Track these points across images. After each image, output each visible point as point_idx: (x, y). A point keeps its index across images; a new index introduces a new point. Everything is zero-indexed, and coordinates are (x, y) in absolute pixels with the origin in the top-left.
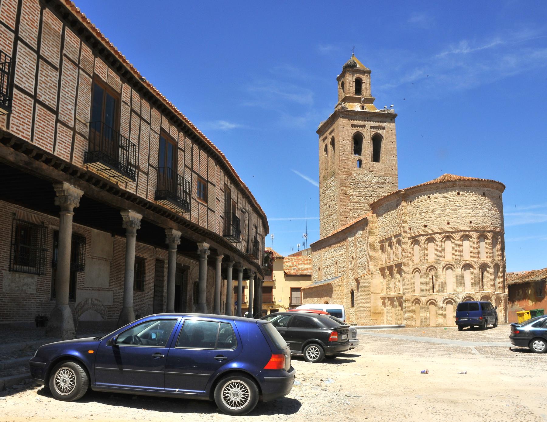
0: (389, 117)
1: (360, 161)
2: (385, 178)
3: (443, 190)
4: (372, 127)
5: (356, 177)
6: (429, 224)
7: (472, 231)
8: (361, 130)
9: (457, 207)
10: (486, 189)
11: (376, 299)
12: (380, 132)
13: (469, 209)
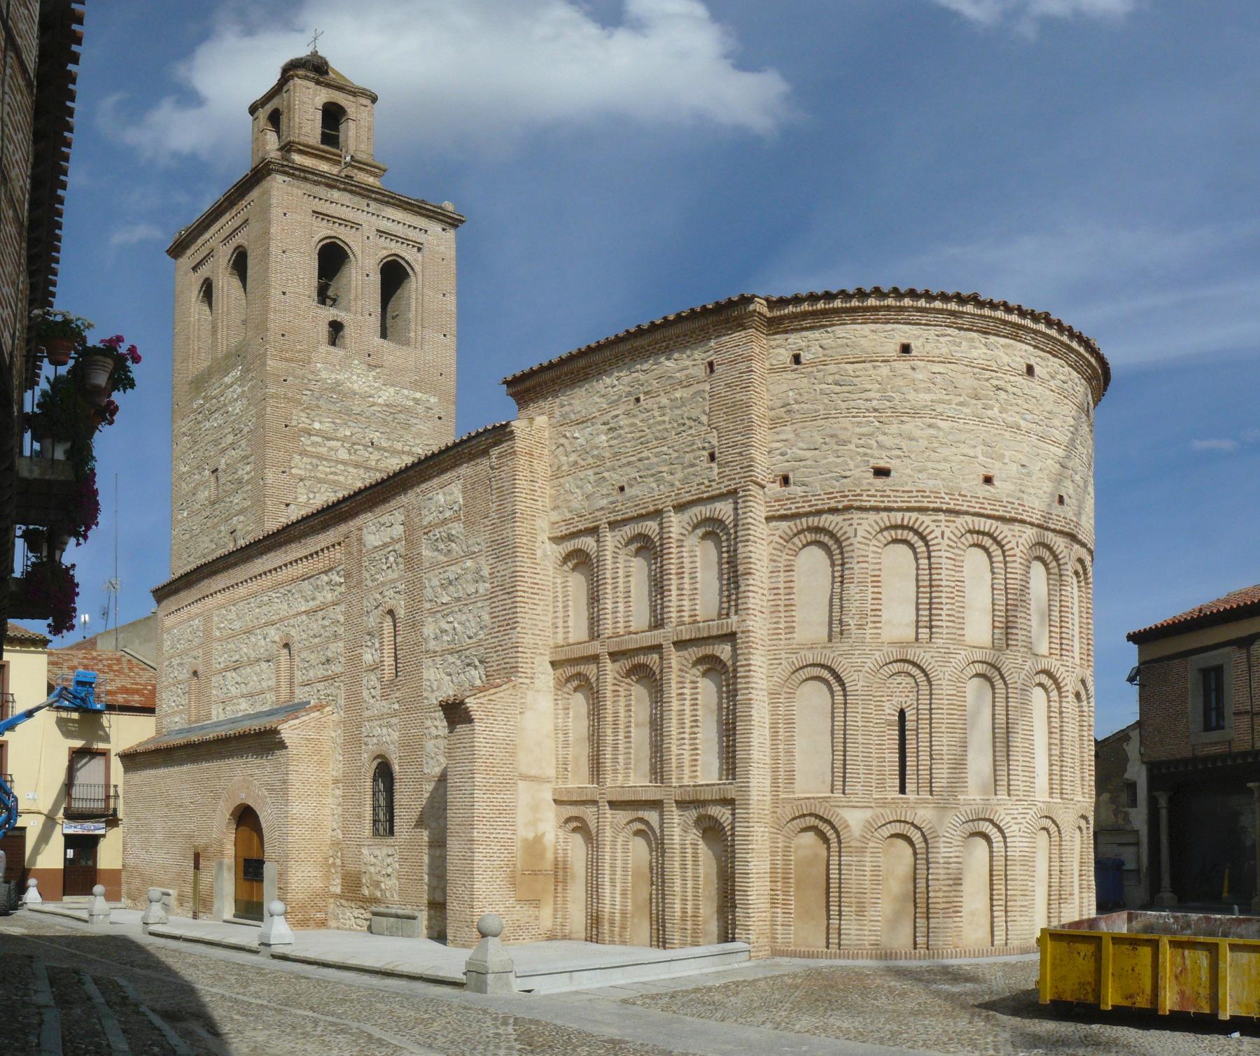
1: (336, 328)
5: (324, 375)
9: (1023, 423)
11: (535, 808)
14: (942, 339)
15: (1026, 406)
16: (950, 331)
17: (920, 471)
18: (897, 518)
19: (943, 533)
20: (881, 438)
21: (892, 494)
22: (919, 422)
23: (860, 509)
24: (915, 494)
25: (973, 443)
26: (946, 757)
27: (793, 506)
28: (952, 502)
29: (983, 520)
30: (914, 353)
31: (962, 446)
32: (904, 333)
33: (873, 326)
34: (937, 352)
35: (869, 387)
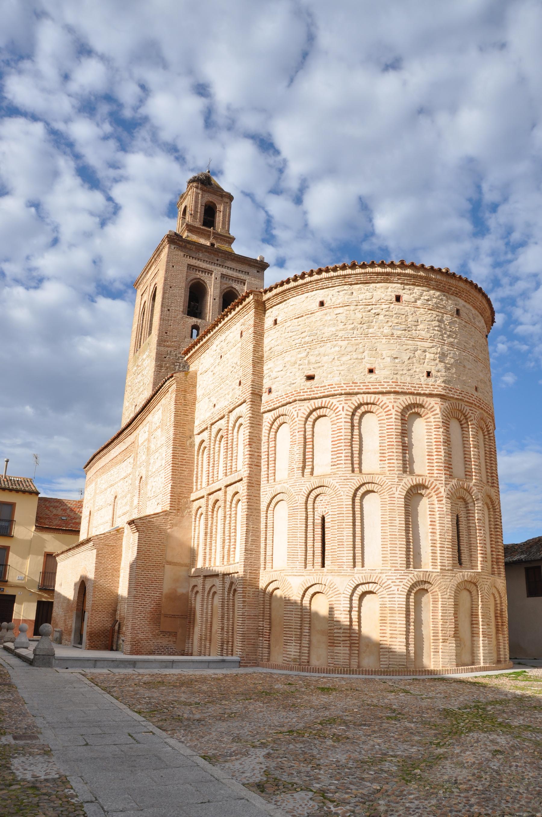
0: (255, 267)
7: (431, 395)
8: (204, 277)
14: (341, 293)
15: (396, 321)
16: (346, 287)
17: (330, 373)
18: (318, 403)
19: (343, 407)
20: (311, 357)
21: (315, 389)
22: (329, 345)
24: (327, 387)
25: (361, 350)
26: (345, 543)
27: (272, 404)
28: (348, 388)
29: (369, 395)
30: (326, 305)
31: (354, 353)
32: (320, 295)
33: (306, 295)
34: (338, 301)
35: (303, 330)
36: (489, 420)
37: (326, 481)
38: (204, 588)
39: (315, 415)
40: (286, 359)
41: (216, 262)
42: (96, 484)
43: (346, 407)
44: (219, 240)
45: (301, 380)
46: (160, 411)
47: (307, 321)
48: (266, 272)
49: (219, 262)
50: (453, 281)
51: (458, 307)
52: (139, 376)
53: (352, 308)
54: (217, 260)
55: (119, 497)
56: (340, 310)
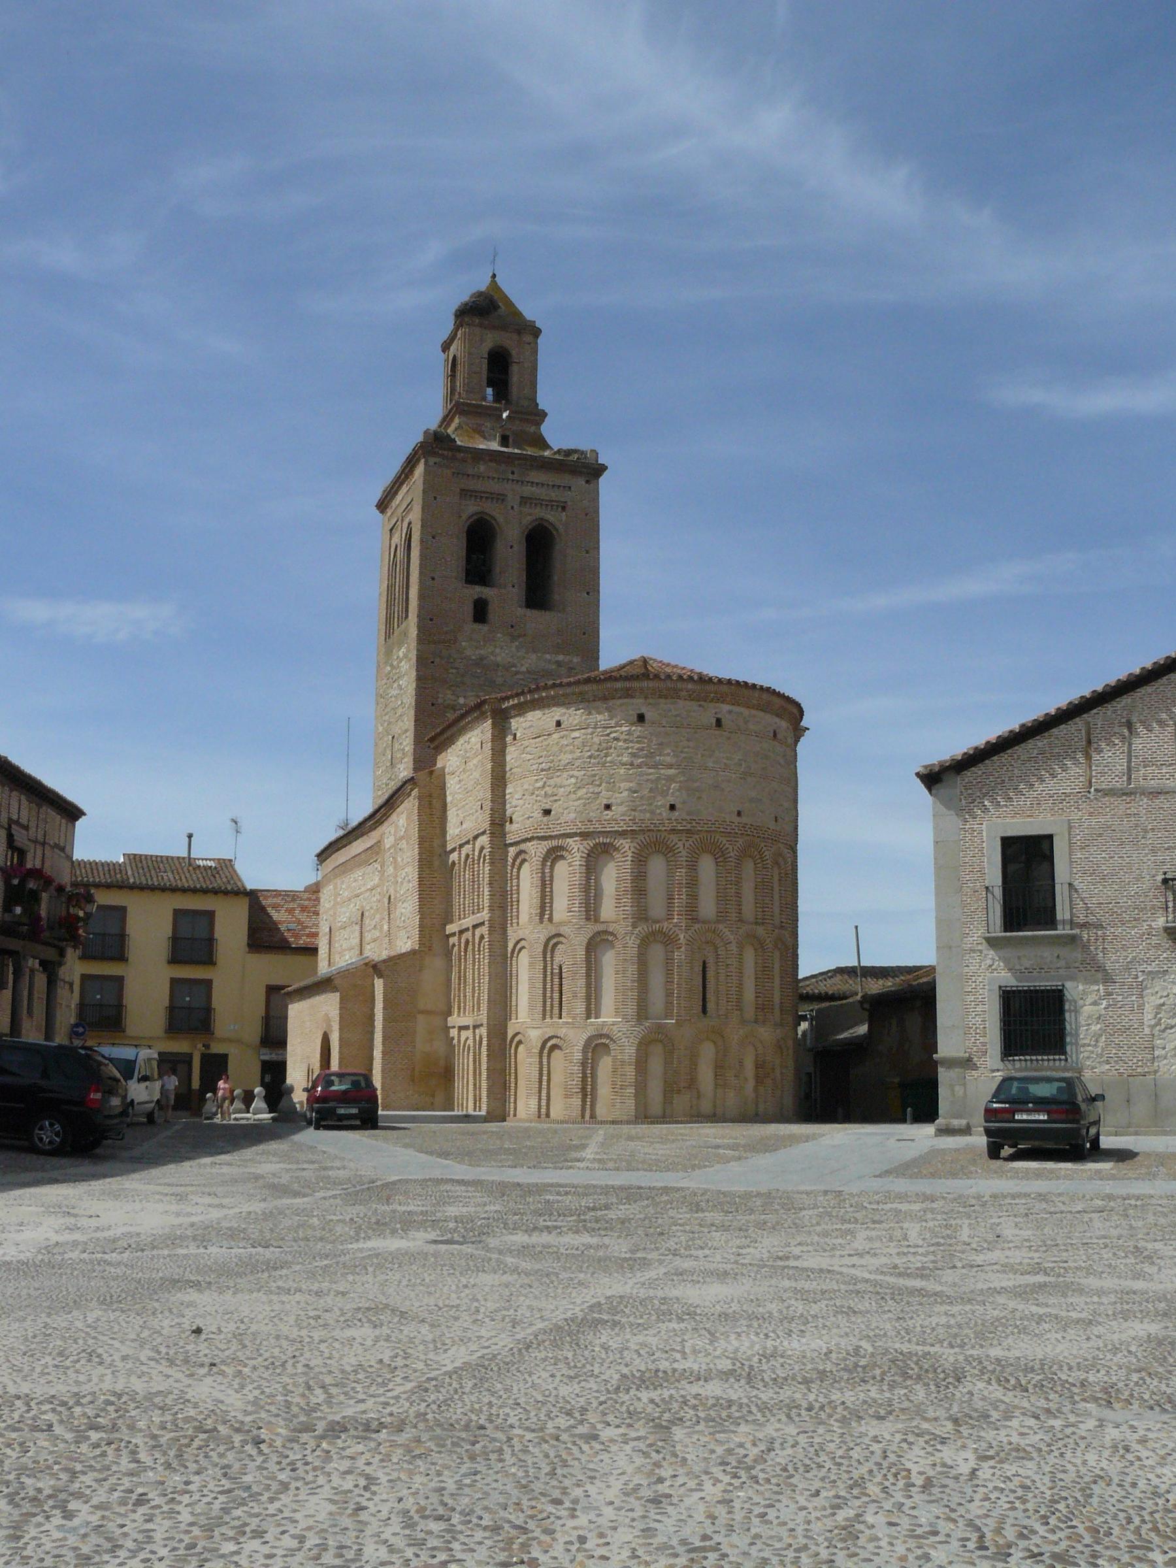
0: (580, 473)
2: (561, 658)
3: (598, 703)
4: (524, 500)
5: (468, 652)
6: (556, 808)
10: (725, 707)
12: (551, 516)
13: (670, 766)
18: (554, 843)
22: (565, 775)
23: (539, 838)
32: (557, 713)
36: (763, 844)
37: (564, 930)
38: (459, 1041)
39: (554, 855)
40: (526, 787)
41: (511, 477)
42: (335, 888)
43: (582, 848)
44: (517, 422)
45: (538, 815)
46: (404, 816)
47: (545, 743)
48: (601, 479)
49: (515, 477)
50: (711, 688)
51: (719, 716)
52: (395, 685)
53: (590, 730)
54: (513, 473)
55: (366, 914)
56: (576, 734)
